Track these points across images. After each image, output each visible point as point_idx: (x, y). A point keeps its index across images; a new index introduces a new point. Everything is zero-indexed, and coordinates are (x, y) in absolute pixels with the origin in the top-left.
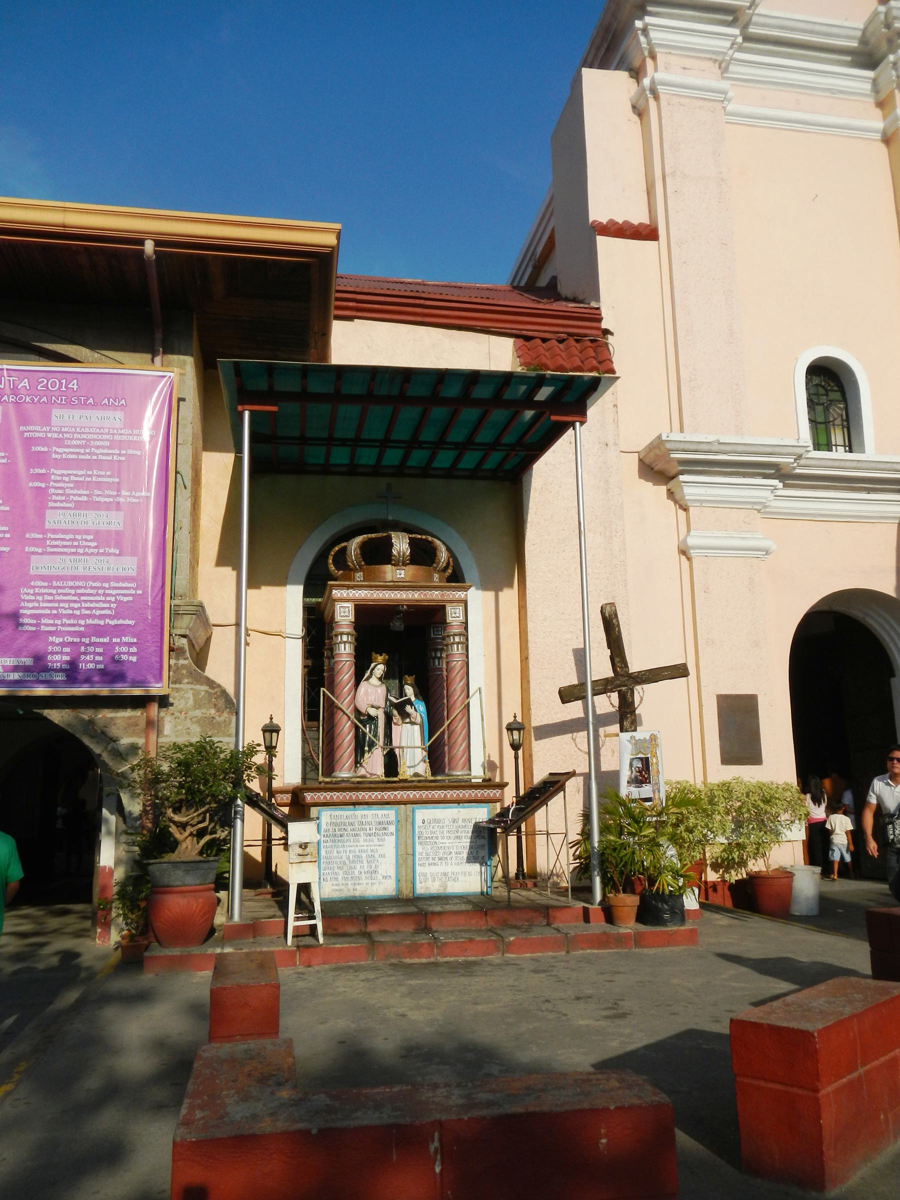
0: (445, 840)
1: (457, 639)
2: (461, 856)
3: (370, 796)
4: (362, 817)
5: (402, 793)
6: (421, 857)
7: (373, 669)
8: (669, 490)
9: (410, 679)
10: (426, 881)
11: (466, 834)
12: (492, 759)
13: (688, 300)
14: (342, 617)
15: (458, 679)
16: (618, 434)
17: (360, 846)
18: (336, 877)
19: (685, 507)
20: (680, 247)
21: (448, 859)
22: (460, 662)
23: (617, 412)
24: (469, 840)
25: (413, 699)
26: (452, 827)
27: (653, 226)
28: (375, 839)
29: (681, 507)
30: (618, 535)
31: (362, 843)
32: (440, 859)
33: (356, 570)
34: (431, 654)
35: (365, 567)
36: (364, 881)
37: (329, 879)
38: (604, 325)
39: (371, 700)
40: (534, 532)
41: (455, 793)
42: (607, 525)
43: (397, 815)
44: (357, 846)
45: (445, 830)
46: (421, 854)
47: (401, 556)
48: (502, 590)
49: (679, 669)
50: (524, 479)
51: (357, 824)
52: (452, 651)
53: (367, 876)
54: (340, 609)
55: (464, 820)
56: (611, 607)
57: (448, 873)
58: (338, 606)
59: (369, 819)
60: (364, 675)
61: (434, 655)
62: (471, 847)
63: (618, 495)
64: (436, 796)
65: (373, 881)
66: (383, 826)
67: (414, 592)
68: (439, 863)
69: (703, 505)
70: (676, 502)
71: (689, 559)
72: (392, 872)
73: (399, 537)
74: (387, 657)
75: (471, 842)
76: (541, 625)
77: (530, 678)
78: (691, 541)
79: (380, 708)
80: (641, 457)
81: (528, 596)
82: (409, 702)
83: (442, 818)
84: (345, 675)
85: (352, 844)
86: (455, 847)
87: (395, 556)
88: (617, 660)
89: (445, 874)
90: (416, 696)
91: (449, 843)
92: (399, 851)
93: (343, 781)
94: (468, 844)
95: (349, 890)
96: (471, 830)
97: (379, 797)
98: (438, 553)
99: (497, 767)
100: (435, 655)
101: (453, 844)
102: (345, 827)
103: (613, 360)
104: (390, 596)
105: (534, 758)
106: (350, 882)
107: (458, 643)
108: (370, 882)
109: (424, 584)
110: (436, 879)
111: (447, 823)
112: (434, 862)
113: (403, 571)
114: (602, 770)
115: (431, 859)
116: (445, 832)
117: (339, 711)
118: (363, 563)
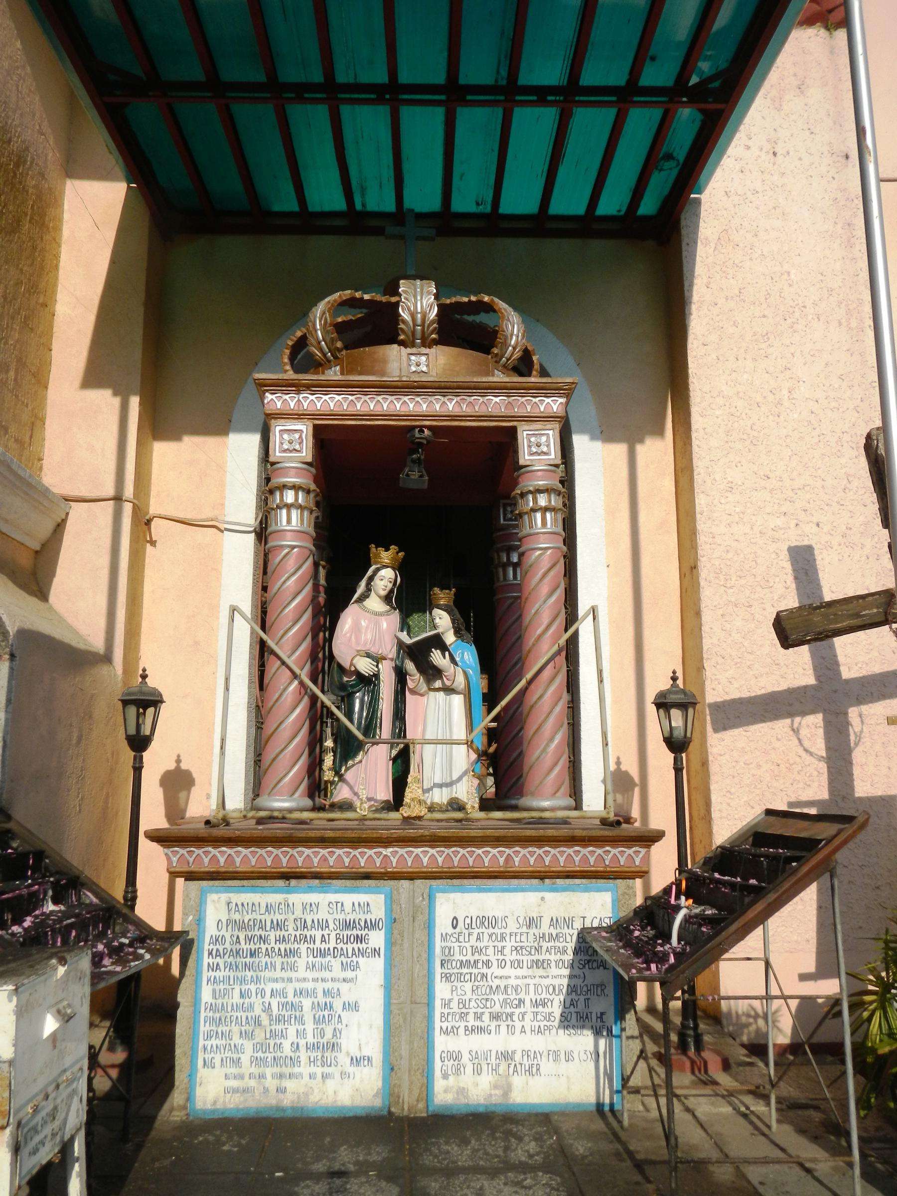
0: (508, 971)
1: (542, 501)
2: (546, 1010)
3: (324, 859)
4: (304, 908)
5: (402, 851)
6: (446, 1011)
7: (371, 579)
9: (443, 596)
10: (458, 1071)
11: (558, 956)
12: (623, 768)
14: (285, 451)
15: (544, 589)
17: (298, 980)
18: (235, 1056)
21: (515, 1018)
22: (549, 552)
24: (566, 972)
25: (450, 638)
26: (524, 938)
28: (336, 964)
31: (302, 973)
32: (495, 1017)
34: (499, 557)
36: (304, 1069)
37: (217, 1061)
39: (366, 643)
41: (532, 854)
42: (851, 307)
43: (391, 903)
44: (290, 980)
45: (509, 944)
46: (446, 1004)
47: (419, 321)
48: (641, 441)
50: (683, 223)
51: (291, 926)
52: (531, 527)
53: (313, 1055)
54: (281, 436)
55: (554, 922)
57: (514, 1052)
59: (322, 914)
60: (355, 592)
61: (505, 560)
62: (572, 989)
64: (486, 861)
65: (326, 1070)
66: (355, 932)
68: (493, 1028)
72: (374, 1048)
73: (415, 286)
74: (401, 554)
75: (571, 977)
76: (723, 501)
77: (703, 605)
79: (385, 659)
81: (695, 443)
82: (437, 642)
83: (499, 914)
84: (288, 578)
85: (278, 974)
86: (532, 988)
87: (404, 322)
89: (506, 1056)
90: (457, 632)
91: (517, 977)
92: (393, 993)
93: (271, 818)
94: (565, 982)
95: (266, 1090)
96: (571, 945)
97: (347, 861)
99: (635, 785)
100: (508, 557)
101: (528, 981)
102: (263, 933)
104: (392, 407)
105: (713, 768)
106: (269, 1072)
107: (545, 510)
108: (319, 1071)
110: (485, 1067)
111: (512, 927)
112: (478, 1023)
113: (424, 358)
114: (857, 795)
115: (471, 1017)
116: (507, 951)
117: (272, 657)
118: (339, 344)
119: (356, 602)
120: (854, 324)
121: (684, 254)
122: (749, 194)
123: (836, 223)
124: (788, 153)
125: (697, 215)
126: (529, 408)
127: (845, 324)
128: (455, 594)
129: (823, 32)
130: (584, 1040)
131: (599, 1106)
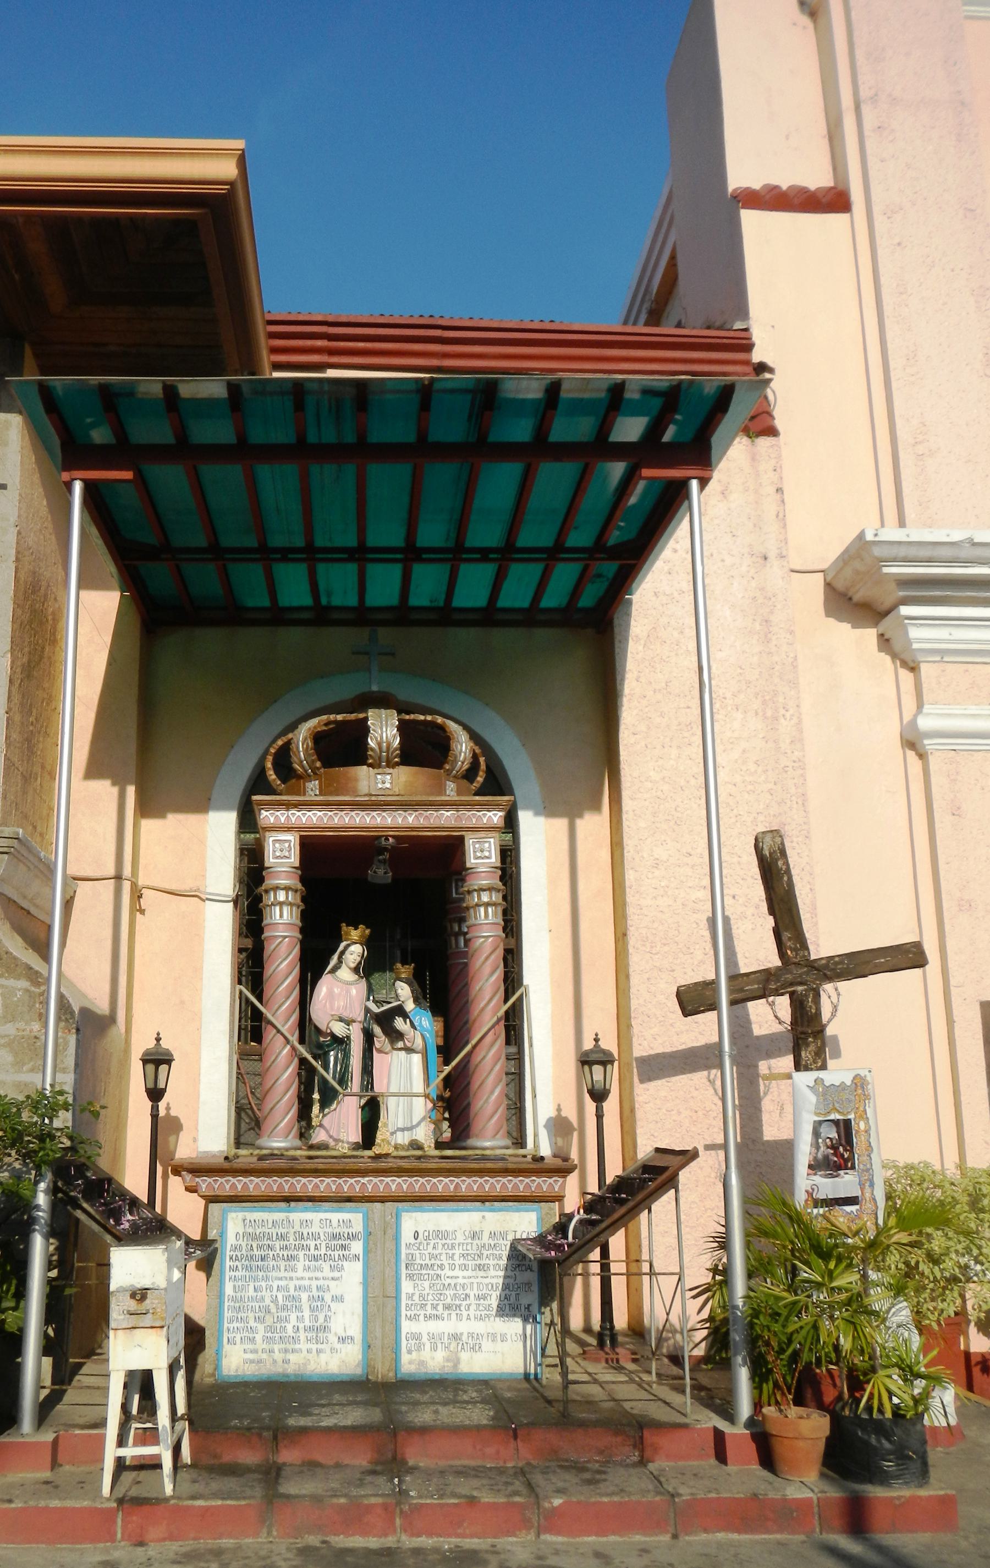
0: (457, 1272)
1: (485, 897)
2: (486, 1302)
3: (316, 1186)
4: (302, 1224)
5: (375, 1180)
6: (410, 1302)
7: (343, 953)
8: (881, 636)
9: (405, 971)
10: (419, 1350)
11: (496, 1262)
13: (907, 306)
14: (277, 857)
15: (487, 968)
16: (786, 539)
17: (298, 1279)
18: (251, 1335)
19: (912, 665)
20: (889, 218)
21: (462, 1308)
22: (491, 939)
23: (783, 501)
24: (502, 1273)
25: (410, 1006)
26: (469, 1247)
27: (840, 187)
28: (326, 1266)
29: (904, 664)
30: (788, 715)
31: (300, 1273)
32: (447, 1307)
33: (307, 778)
34: (452, 928)
35: (322, 770)
36: (303, 1346)
37: (238, 1340)
38: (757, 356)
40: (635, 712)
41: (475, 1182)
42: (767, 698)
43: (367, 1220)
44: (291, 1279)
45: (457, 1252)
46: (410, 1297)
47: (384, 748)
48: (581, 816)
49: (908, 951)
50: (616, 622)
51: (292, 1238)
52: (476, 918)
53: (310, 1335)
54: (274, 845)
55: (492, 1235)
56: (774, 838)
57: (461, 1334)
58: (271, 839)
59: (315, 1229)
61: (457, 929)
62: (506, 1287)
63: (788, 644)
64: (440, 1187)
65: (320, 1346)
66: (340, 1242)
67: (406, 814)
68: (445, 1316)
69: (944, 660)
70: (894, 656)
71: (922, 756)
72: (355, 1329)
73: (380, 717)
74: (368, 931)
75: (505, 1277)
76: (650, 876)
77: (631, 970)
78: (924, 723)
79: (355, 1022)
80: (828, 579)
81: (625, 823)
82: (400, 1011)
83: (450, 1229)
84: (281, 962)
85: (282, 1274)
86: (475, 1285)
87: (372, 749)
88: (786, 935)
89: (456, 1337)
90: (416, 1000)
91: (464, 1278)
92: (370, 1290)
94: (501, 1281)
95: (275, 1361)
96: (505, 1253)
97: (334, 1187)
98: (453, 745)
99: (574, 1129)
100: (460, 928)
101: (472, 1280)
102: (270, 1243)
103: (775, 413)
104: (364, 821)
105: (639, 1114)
106: (276, 1347)
107: (487, 905)
108: (314, 1347)
109: (424, 798)
110: (439, 1345)
111: (460, 1239)
112: (435, 1312)
113: (388, 777)
114: (765, 1138)
115: (429, 1307)
116: (456, 1257)
117: (269, 1027)
118: (318, 764)
119: (329, 972)
120: (769, 713)
121: (617, 650)
122: (676, 594)
123: (754, 620)
124: (712, 555)
125: (628, 615)
126: (474, 820)
127: (761, 714)
128: (414, 969)
129: (745, 440)
130: (515, 1326)
131: (526, 1376)
